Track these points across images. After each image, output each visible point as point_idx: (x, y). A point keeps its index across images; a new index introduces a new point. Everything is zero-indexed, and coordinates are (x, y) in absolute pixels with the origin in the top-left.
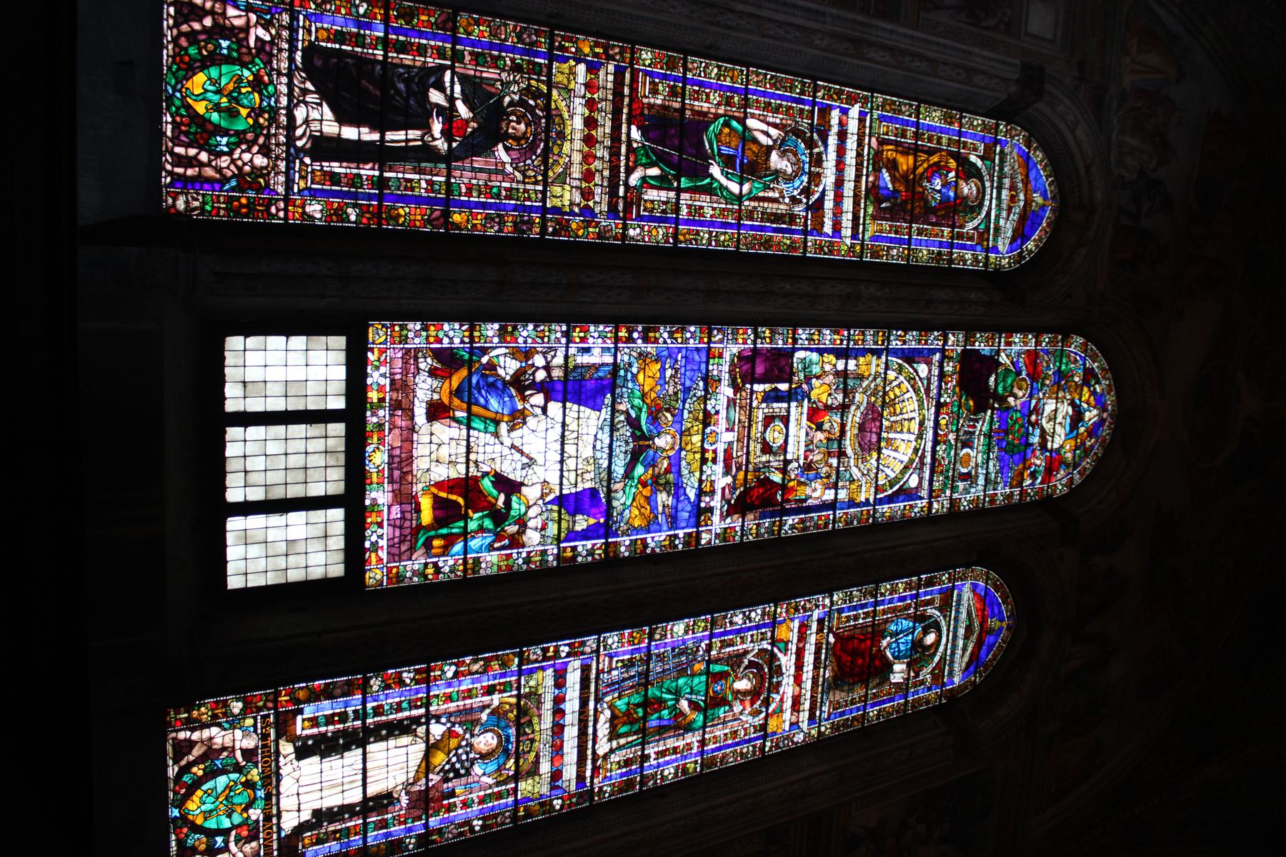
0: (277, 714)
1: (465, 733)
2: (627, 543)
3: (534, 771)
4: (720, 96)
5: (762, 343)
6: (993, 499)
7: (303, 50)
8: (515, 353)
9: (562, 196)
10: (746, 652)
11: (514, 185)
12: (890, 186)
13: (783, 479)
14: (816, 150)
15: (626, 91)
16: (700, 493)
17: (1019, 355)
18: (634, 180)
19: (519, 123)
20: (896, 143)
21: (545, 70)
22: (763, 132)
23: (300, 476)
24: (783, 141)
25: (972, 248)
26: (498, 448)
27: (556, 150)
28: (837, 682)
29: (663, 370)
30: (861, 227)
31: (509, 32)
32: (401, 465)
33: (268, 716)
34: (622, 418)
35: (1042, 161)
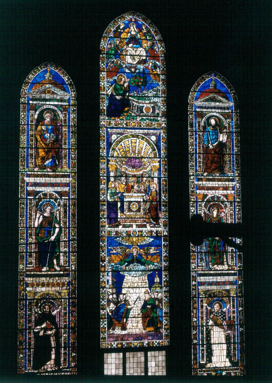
0: (199, 368)
1: (213, 314)
2: (164, 263)
3: (228, 291)
4: (29, 238)
5: (105, 215)
6: (164, 92)
7: (34, 370)
8: (109, 305)
9: (65, 293)
10: (205, 213)
11: (63, 308)
12: (50, 160)
13: (149, 202)
14: (42, 196)
15: (32, 273)
16: (152, 237)
17: (108, 82)
18: (58, 268)
19: (45, 308)
20: (35, 158)
21: (30, 301)
22: (39, 220)
23: (139, 364)
24: (41, 211)
25: (69, 115)
26: (134, 308)
27: (52, 296)
28: (221, 170)
29: (113, 254)
30: (66, 173)
31: (21, 313)
32: (138, 337)
33: (199, 370)
34: (127, 267)
35: (33, 75)
